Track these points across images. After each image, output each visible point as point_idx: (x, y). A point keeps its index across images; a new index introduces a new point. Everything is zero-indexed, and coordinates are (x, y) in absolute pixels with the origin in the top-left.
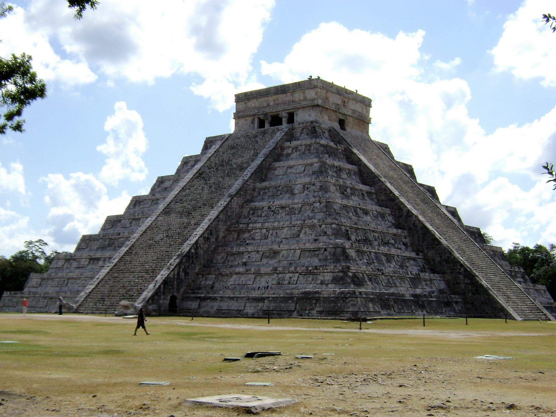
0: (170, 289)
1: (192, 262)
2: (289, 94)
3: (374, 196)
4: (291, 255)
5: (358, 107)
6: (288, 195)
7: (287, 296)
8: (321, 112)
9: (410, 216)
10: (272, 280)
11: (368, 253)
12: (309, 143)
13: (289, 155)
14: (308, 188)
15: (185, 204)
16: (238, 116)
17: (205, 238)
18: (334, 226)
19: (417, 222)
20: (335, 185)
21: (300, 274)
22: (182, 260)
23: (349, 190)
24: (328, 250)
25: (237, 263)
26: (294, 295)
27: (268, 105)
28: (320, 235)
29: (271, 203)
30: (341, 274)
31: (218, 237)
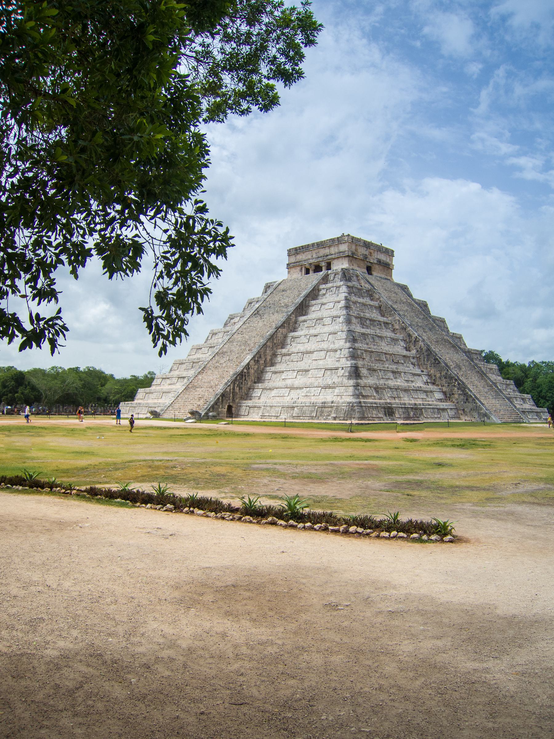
1: (245, 379)
5: (383, 257)
8: (351, 261)
9: (418, 341)
11: (379, 371)
13: (324, 295)
14: (335, 320)
15: (244, 335)
17: (255, 361)
19: (423, 345)
20: (356, 318)
23: (368, 322)
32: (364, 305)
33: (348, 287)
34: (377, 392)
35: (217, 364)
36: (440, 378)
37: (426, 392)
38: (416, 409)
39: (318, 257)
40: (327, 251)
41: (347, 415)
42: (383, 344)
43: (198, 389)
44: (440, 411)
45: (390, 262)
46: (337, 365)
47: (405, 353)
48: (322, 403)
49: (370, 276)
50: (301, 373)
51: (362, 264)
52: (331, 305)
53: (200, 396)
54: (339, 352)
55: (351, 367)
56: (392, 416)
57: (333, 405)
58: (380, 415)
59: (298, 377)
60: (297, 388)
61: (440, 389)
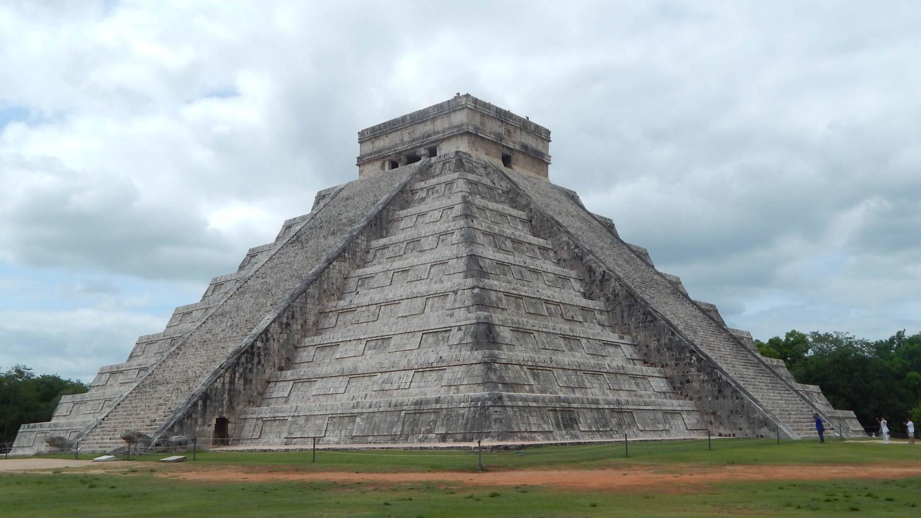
0: (215, 408)
1: (259, 363)
2: (428, 123)
3: (552, 254)
5: (531, 142)
8: (474, 143)
9: (607, 280)
13: (423, 199)
14: (443, 241)
15: (268, 279)
16: (362, 162)
17: (281, 324)
18: (476, 291)
19: (619, 288)
20: (485, 233)
22: (239, 358)
23: (509, 244)
31: (305, 322)
32: (502, 215)
33: (469, 182)
34: (536, 376)
35: (208, 336)
36: (659, 351)
37: (634, 377)
38: (620, 412)
39: (414, 140)
40: (428, 128)
41: (472, 428)
42: (541, 285)
43: (160, 388)
44: (669, 416)
45: (543, 151)
46: (451, 322)
47: (584, 302)
48: (416, 404)
49: (509, 170)
50: (373, 344)
51: (493, 149)
52: (437, 214)
53: (161, 401)
54: (451, 297)
55: (478, 323)
56: (572, 428)
57: (438, 406)
58: (546, 427)
60: (363, 375)
61: (660, 372)
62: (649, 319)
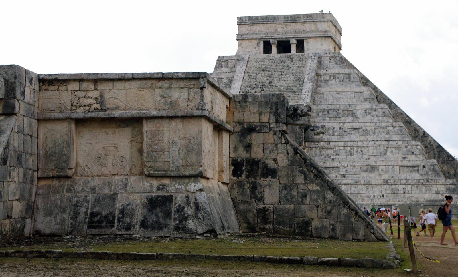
2: (299, 24)
4: (390, 170)
6: (350, 119)
7: (413, 203)
9: (426, 137)
10: (387, 190)
12: (347, 72)
16: (241, 38)
19: (433, 142)
21: (413, 185)
24: (427, 166)
25: (334, 176)
26: (421, 203)
27: (276, 30)
28: (408, 154)
29: (341, 124)
30: (453, 187)
59: (361, 173)
62: (450, 159)
